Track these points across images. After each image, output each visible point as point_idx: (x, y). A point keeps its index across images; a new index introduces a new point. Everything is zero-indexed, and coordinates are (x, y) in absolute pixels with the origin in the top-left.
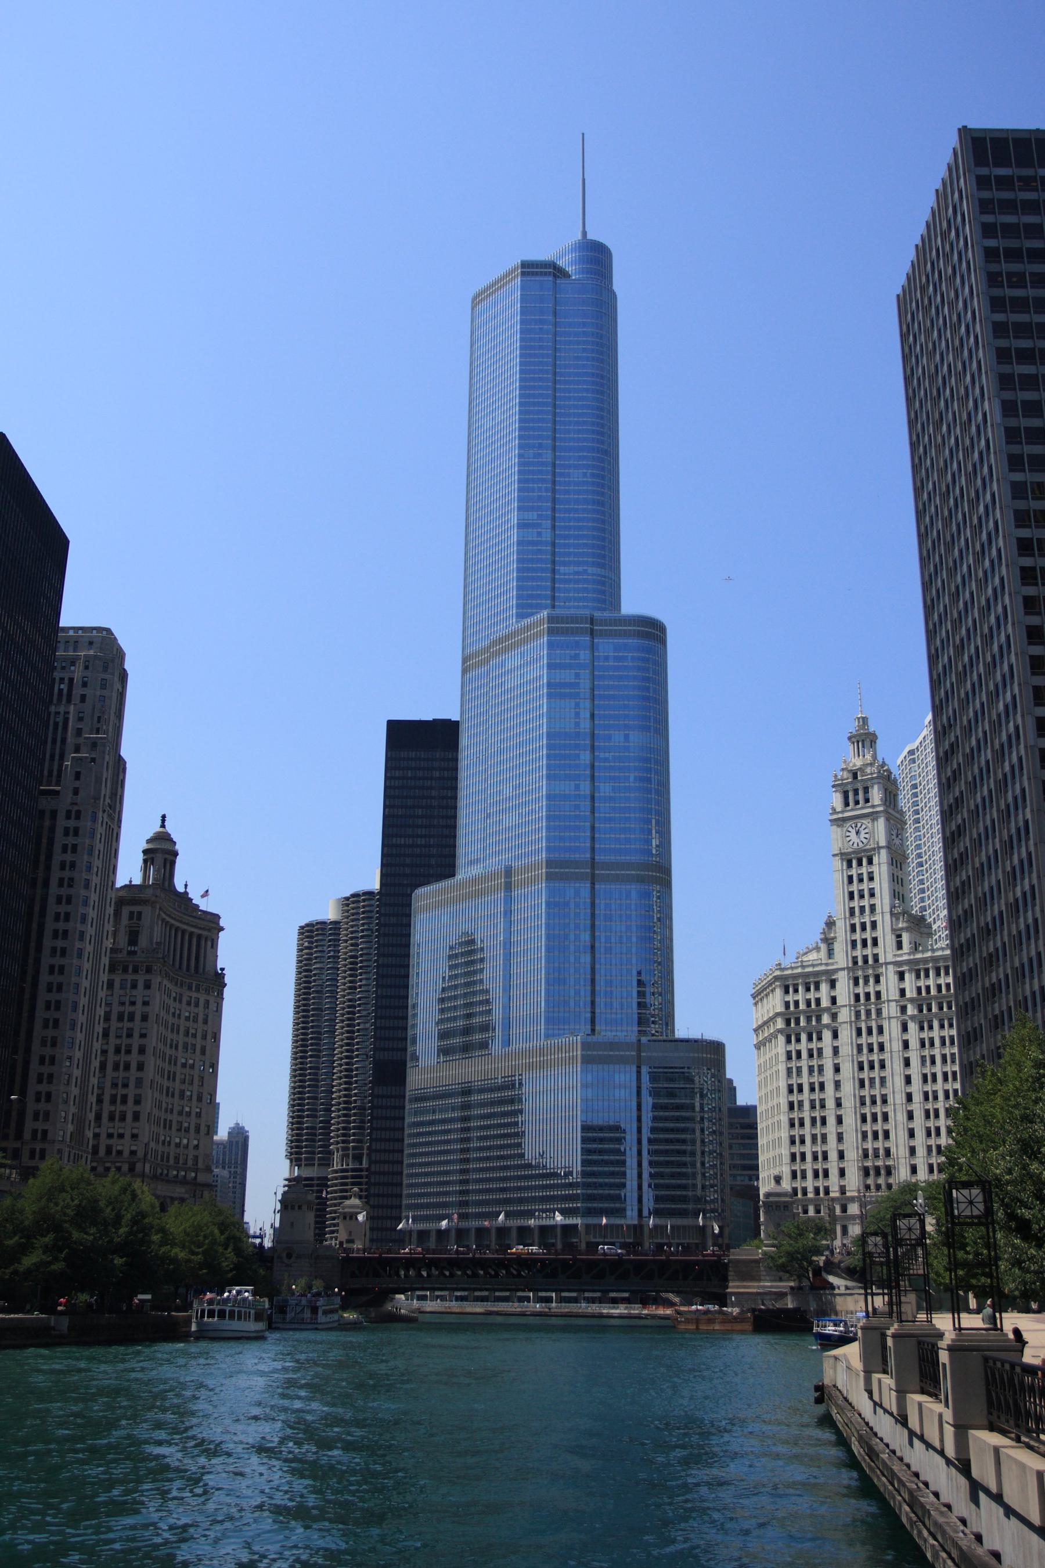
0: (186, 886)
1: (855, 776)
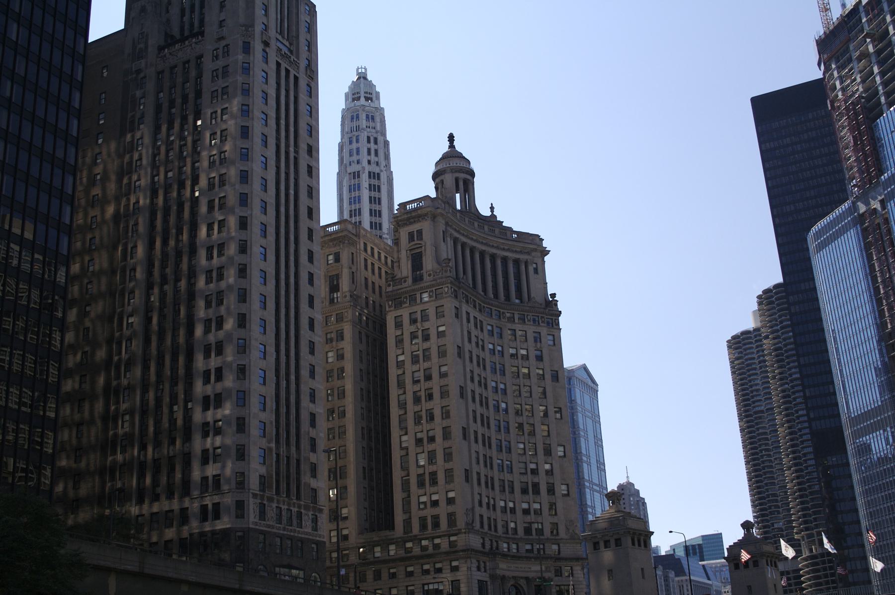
0: (492, 208)
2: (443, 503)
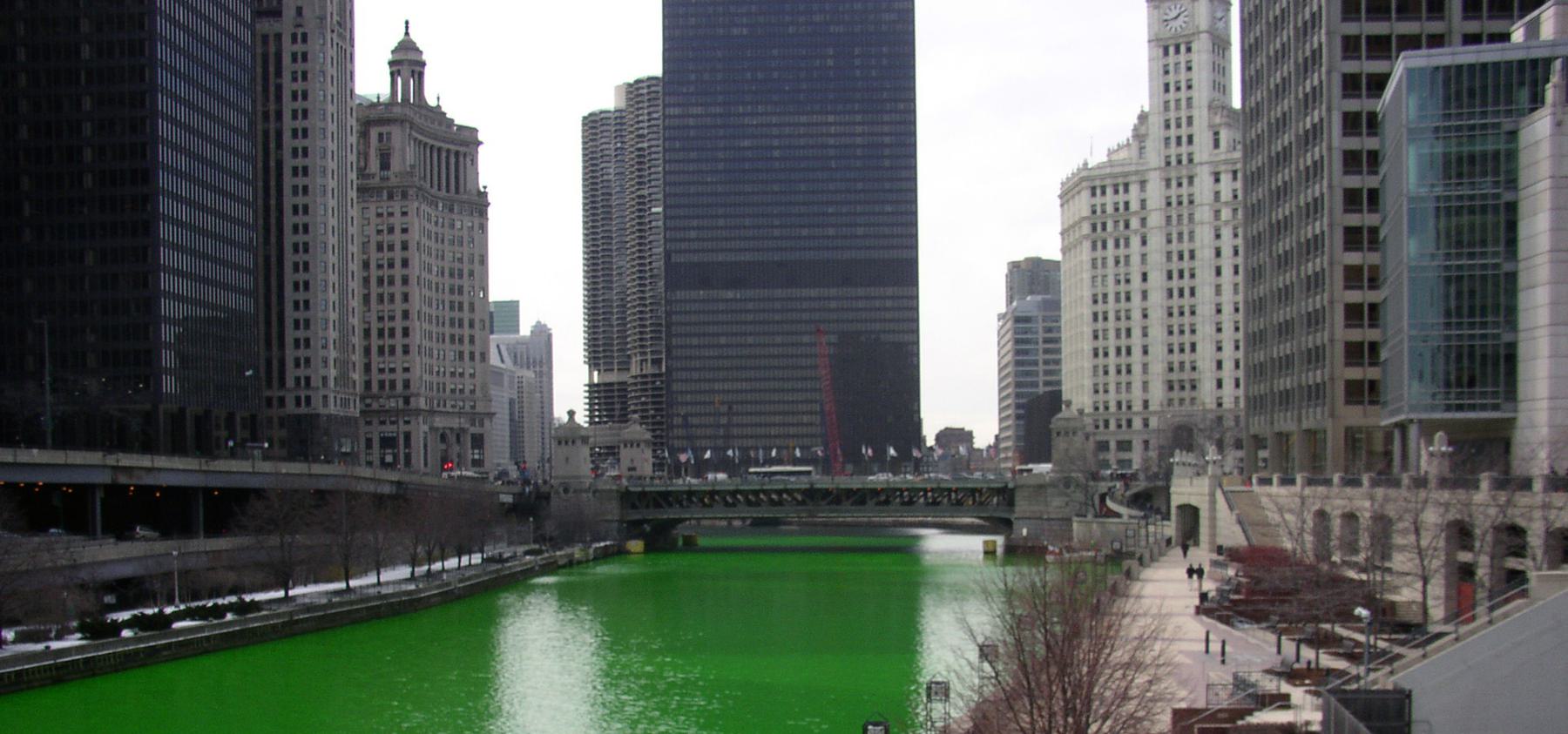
2: (399, 370)
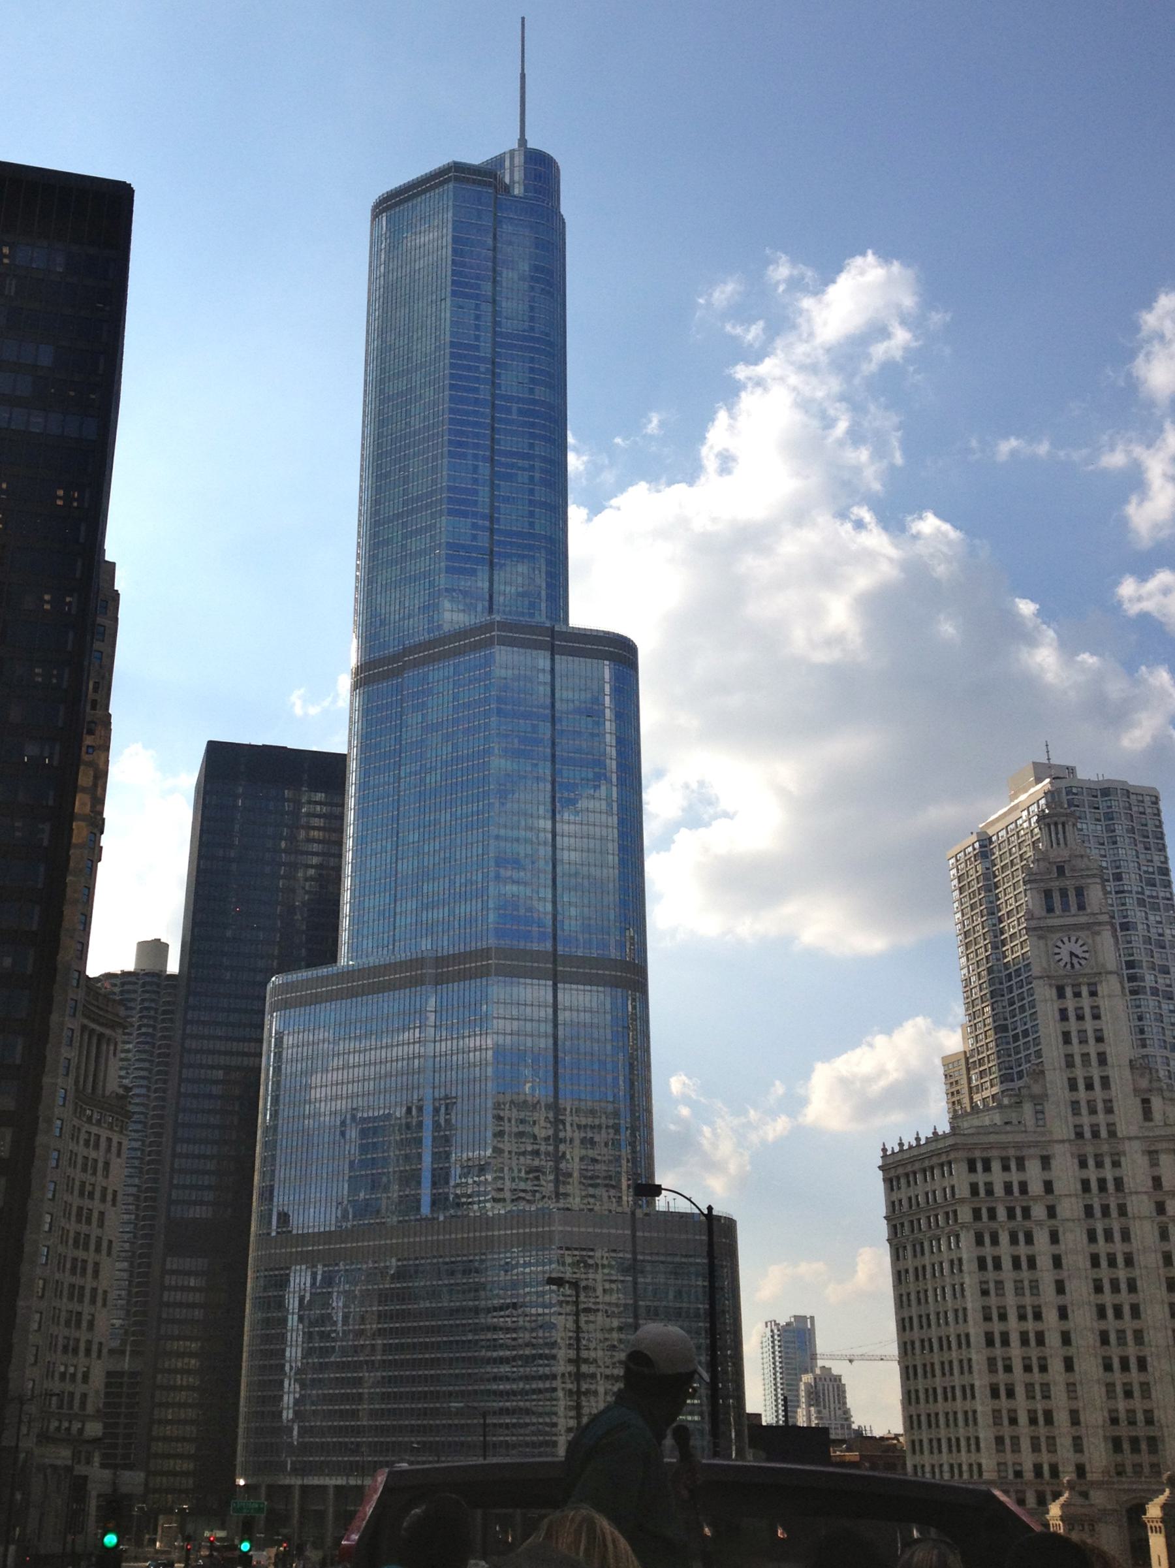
1: (1061, 870)
